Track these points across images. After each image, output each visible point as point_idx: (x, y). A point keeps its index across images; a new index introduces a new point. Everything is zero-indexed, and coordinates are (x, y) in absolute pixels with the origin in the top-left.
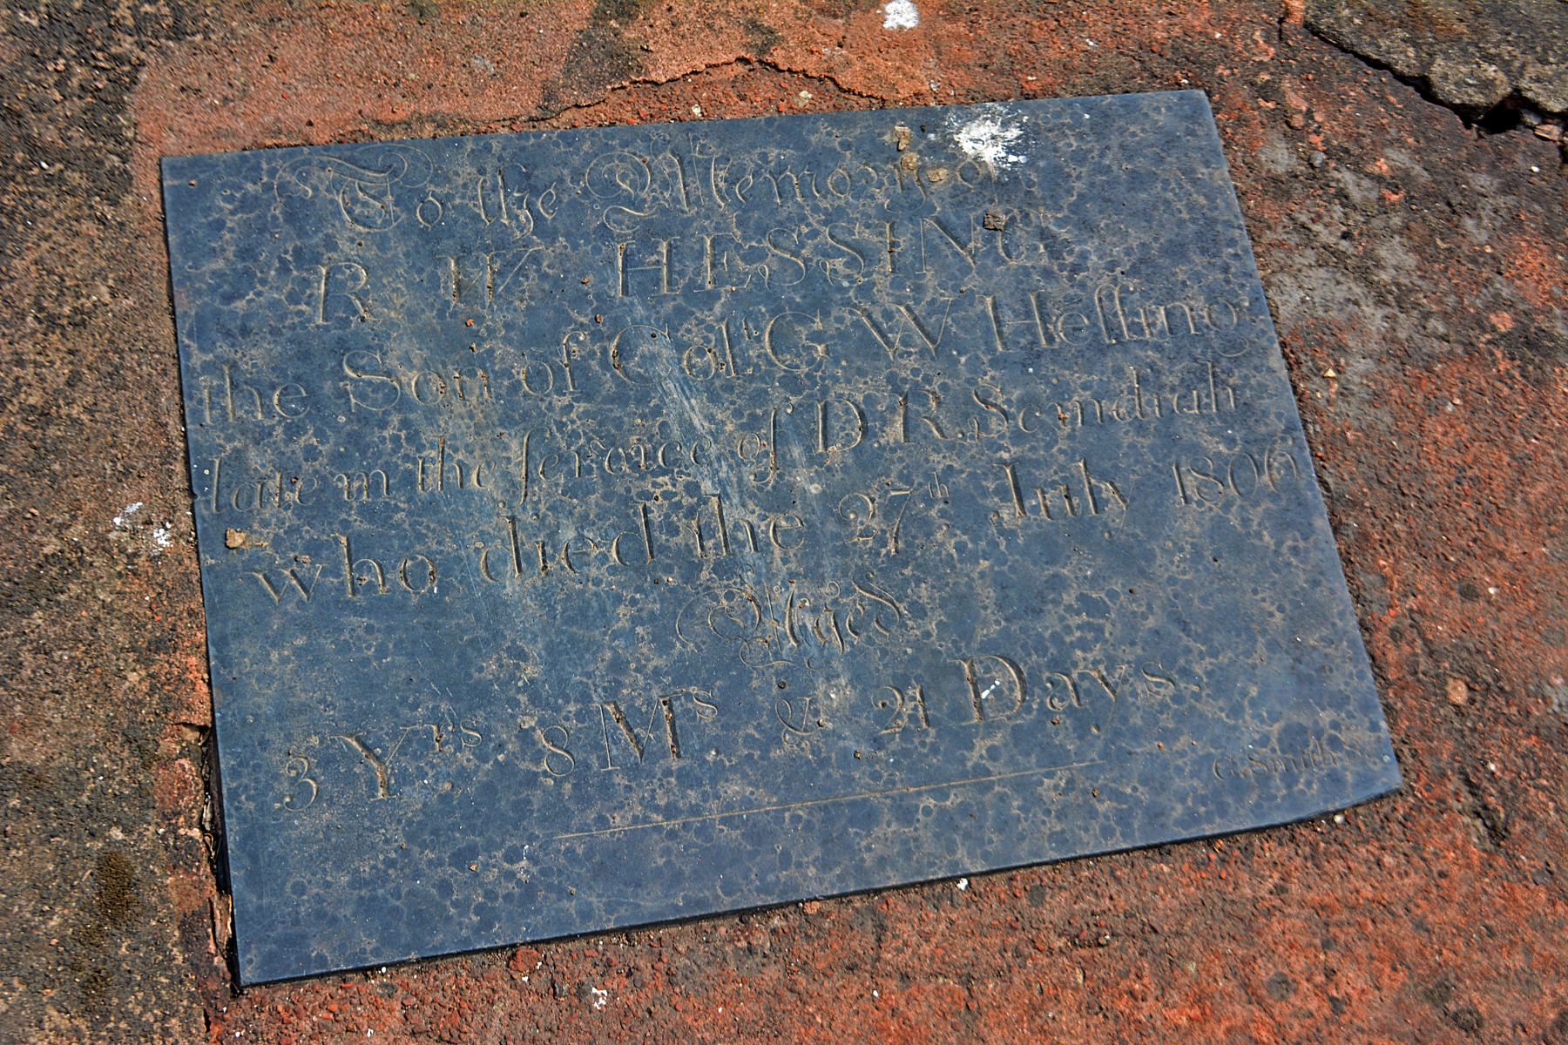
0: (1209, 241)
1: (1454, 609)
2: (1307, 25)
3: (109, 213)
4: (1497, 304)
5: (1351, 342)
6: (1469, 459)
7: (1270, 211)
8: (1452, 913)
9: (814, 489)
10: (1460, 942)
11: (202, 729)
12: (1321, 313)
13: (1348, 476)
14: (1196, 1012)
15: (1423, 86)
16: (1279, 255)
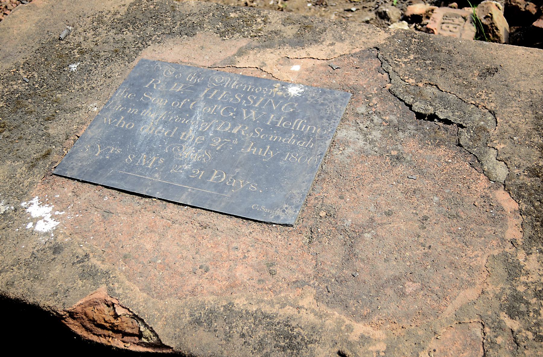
0: (329, 119)
1: (336, 199)
2: (389, 90)
3: (127, 63)
4: (396, 149)
5: (352, 146)
6: (363, 174)
7: (352, 119)
8: (286, 252)
9: (211, 135)
10: (283, 258)
11: (78, 137)
12: (348, 138)
13: (329, 168)
14: (214, 246)
15: (410, 107)
16: (346, 126)
